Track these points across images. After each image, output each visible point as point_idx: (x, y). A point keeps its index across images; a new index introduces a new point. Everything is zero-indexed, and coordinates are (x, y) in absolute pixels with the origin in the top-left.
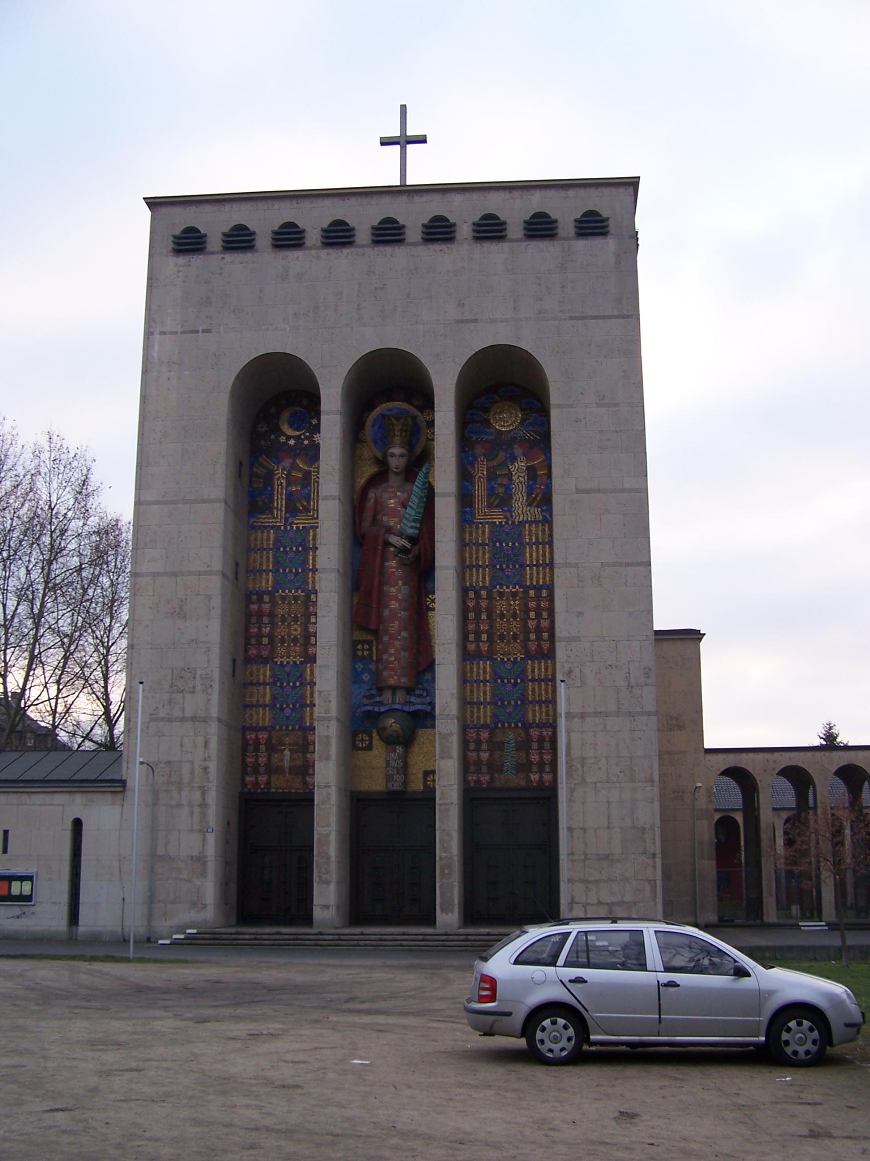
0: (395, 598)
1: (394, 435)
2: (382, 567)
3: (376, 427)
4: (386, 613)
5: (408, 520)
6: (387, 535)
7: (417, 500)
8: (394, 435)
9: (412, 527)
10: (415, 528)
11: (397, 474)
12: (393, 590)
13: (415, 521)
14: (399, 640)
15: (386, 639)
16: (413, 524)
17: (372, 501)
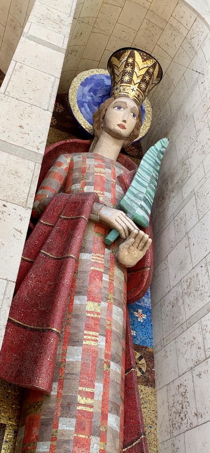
0: (95, 324)
1: (130, 82)
2: (77, 261)
3: (87, 89)
4: (75, 356)
5: (135, 196)
6: (96, 206)
7: (149, 178)
8: (130, 82)
9: (142, 207)
10: (146, 211)
11: (116, 136)
12: (90, 306)
13: (145, 200)
14: (103, 437)
15: (66, 426)
16: (143, 203)
17: (65, 166)
